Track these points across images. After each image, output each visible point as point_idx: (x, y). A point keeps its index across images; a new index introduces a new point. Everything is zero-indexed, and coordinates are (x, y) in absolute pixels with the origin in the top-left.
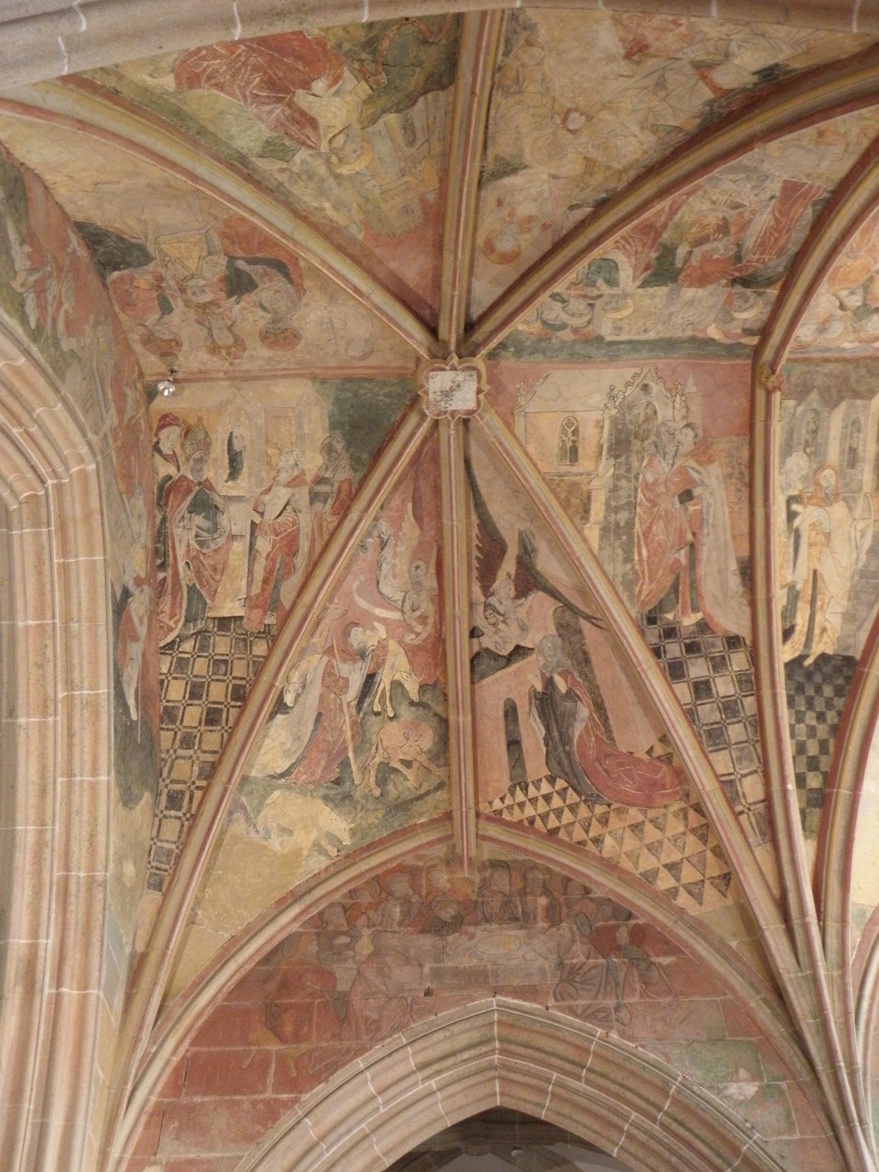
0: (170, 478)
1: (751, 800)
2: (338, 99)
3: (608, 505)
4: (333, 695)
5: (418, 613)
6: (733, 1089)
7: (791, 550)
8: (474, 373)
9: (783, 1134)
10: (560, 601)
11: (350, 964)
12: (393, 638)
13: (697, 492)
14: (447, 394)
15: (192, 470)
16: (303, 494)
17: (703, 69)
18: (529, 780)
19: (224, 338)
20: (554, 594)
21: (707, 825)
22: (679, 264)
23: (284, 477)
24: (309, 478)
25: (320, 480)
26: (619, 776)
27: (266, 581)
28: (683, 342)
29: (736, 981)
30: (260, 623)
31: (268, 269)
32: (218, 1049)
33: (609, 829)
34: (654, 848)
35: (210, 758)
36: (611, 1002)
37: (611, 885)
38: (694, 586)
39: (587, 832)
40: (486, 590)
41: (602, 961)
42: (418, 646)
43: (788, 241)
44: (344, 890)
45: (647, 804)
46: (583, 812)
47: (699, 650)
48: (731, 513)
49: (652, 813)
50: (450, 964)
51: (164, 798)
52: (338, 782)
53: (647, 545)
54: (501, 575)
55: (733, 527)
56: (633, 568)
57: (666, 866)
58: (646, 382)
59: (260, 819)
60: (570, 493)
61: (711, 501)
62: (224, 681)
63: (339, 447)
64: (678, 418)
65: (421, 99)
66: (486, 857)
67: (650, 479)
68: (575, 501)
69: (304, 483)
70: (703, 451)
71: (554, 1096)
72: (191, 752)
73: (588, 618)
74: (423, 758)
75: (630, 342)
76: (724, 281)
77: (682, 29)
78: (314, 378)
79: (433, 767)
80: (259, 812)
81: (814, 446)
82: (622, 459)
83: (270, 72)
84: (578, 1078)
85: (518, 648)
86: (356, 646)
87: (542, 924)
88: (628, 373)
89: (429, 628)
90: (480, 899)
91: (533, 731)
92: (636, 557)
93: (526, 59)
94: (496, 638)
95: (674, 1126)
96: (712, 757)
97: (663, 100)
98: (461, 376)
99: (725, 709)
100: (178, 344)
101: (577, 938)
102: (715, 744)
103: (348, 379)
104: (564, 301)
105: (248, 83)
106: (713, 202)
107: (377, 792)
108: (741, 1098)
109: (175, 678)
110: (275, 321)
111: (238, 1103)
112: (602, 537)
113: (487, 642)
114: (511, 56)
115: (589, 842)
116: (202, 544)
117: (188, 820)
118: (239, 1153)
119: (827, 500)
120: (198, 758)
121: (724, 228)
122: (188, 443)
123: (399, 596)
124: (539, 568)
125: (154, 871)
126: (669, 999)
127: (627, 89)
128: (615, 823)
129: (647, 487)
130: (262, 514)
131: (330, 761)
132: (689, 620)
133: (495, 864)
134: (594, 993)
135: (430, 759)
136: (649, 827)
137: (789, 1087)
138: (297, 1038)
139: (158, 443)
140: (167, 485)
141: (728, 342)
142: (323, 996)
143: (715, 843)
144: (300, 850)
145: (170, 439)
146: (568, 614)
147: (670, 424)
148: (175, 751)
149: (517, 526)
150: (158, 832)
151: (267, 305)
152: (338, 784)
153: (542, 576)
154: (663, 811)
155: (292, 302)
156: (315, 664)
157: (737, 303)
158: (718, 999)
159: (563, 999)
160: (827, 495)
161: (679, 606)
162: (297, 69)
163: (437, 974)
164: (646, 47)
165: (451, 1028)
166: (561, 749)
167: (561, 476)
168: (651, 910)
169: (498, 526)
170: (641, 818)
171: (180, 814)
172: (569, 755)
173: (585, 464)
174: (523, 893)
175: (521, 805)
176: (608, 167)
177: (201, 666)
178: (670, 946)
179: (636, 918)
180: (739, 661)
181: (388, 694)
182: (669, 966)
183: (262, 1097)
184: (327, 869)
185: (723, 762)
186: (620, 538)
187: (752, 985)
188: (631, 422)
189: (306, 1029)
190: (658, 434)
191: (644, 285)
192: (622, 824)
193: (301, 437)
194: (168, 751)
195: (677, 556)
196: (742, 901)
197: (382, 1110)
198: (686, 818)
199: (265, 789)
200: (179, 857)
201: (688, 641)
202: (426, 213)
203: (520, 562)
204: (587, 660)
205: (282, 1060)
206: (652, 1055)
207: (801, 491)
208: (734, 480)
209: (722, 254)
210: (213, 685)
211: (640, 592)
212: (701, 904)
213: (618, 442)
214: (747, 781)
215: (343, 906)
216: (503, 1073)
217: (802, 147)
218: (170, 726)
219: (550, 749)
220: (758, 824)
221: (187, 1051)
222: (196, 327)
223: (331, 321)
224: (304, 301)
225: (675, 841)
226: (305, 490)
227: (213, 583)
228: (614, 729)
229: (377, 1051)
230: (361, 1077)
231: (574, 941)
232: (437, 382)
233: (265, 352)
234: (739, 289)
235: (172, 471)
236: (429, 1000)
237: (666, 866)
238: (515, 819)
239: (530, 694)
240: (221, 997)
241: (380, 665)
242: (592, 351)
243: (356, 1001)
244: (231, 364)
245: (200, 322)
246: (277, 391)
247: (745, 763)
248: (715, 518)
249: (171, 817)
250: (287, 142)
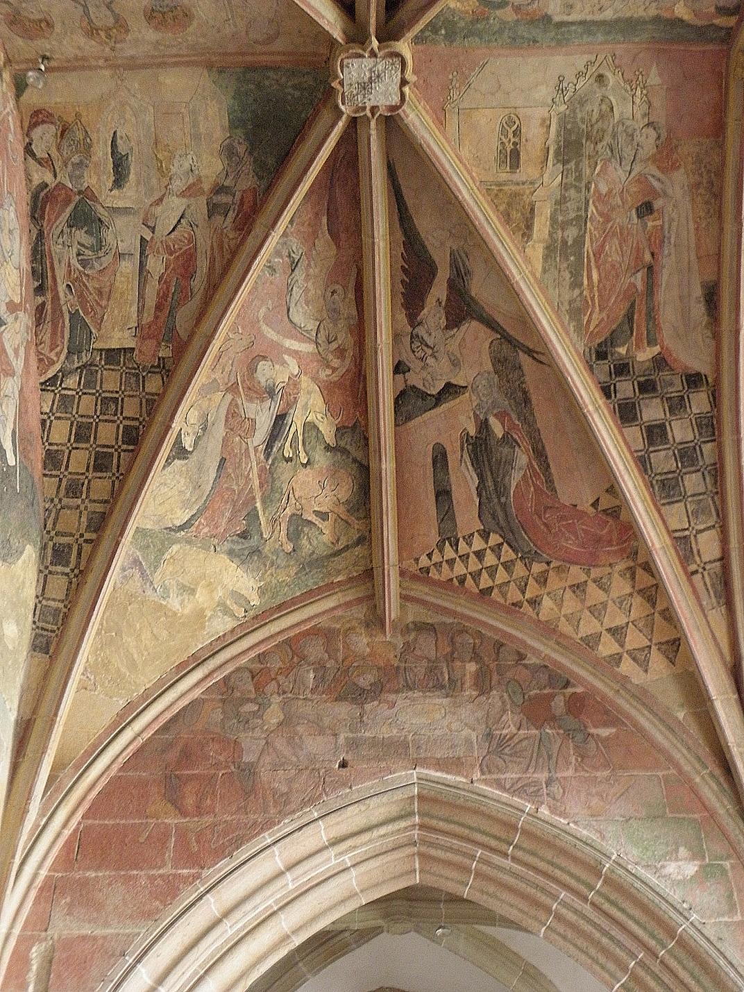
0: (47, 185)
1: (706, 558)
3: (553, 220)
4: (238, 439)
5: (334, 345)
6: (671, 868)
8: (397, 61)
9: (723, 915)
10: (497, 332)
11: (257, 733)
12: (306, 374)
13: (657, 204)
14: (365, 87)
15: (70, 177)
16: (199, 206)
18: (460, 535)
19: (102, 17)
20: (491, 324)
21: (657, 586)
23: (178, 185)
24: (206, 187)
25: (219, 189)
26: (560, 530)
27: (159, 307)
28: (644, 22)
29: (681, 755)
30: (154, 355)
32: (112, 822)
33: (547, 590)
34: (597, 611)
35: (99, 508)
36: (542, 776)
37: (548, 651)
38: (651, 315)
39: (523, 593)
40: (413, 319)
41: (534, 732)
42: (335, 383)
44: (252, 654)
45: (590, 562)
46: (519, 570)
47: (654, 389)
48: (697, 229)
49: (595, 573)
50: (367, 734)
51: (50, 551)
52: (244, 535)
53: (598, 267)
54: (431, 301)
55: (698, 247)
56: (581, 293)
57: (609, 630)
59: (157, 577)
60: (509, 204)
61: (674, 215)
62: (114, 422)
63: (241, 149)
64: (638, 116)
66: (410, 619)
67: (604, 189)
68: (516, 215)
69: (203, 193)
70: (666, 156)
71: (478, 874)
72: (79, 501)
73: (530, 352)
74: (342, 510)
78: (209, 66)
79: (352, 519)
80: (156, 568)
82: (572, 165)
84: (505, 855)
85: (449, 385)
86: (263, 383)
87: (470, 692)
88: (580, 61)
89: (348, 361)
90: (403, 665)
91: (464, 480)
92: (585, 282)
94: (424, 374)
95: (606, 906)
96: (663, 509)
99: (681, 457)
101: (508, 706)
102: (668, 496)
103: (251, 68)
107: (289, 547)
108: (680, 877)
109: (59, 418)
111: (136, 878)
112: (546, 258)
113: (414, 379)
115: (525, 603)
116: (84, 263)
117: (76, 576)
118: (137, 930)
120: (86, 508)
122: (65, 143)
123: (312, 326)
124: (473, 294)
125: (40, 631)
126: (606, 773)
128: (554, 582)
129: (600, 198)
130: (153, 230)
131: (234, 514)
132: (645, 355)
133: (420, 627)
134: (524, 766)
135: (348, 511)
136: (592, 587)
137: (733, 867)
138: (199, 811)
139: (31, 144)
140: (42, 194)
141: (699, 23)
142: (227, 767)
143: (665, 605)
144: (203, 610)
145: (44, 138)
146: (506, 348)
147: (628, 123)
148: (60, 500)
149: (448, 244)
150: (44, 590)
152: (245, 538)
153: (477, 304)
154: (608, 570)
156: (219, 403)
158: (660, 774)
159: (490, 772)
161: (633, 338)
163: (353, 744)
165: (367, 801)
166: (496, 500)
167: (500, 185)
168: (591, 679)
169: (426, 243)
170: (583, 577)
171: (67, 570)
172: (504, 507)
173: (528, 171)
174: (450, 658)
175: (451, 562)
177: (87, 405)
178: (610, 716)
179: (574, 686)
180: (699, 402)
181: (301, 438)
182: (607, 738)
183: (161, 871)
184: (233, 630)
185: (677, 516)
186: (567, 259)
187: (699, 759)
188: (583, 120)
189: (209, 801)
190: (614, 136)
192: (563, 584)
193: (197, 137)
194: (52, 500)
195: (633, 279)
196: (691, 669)
197: (291, 887)
198: (633, 578)
199: (163, 544)
200: (66, 616)
201: (642, 379)
203: (451, 285)
204: (527, 401)
205: (182, 834)
206: (585, 832)
208: (701, 191)
210: (101, 425)
211: (589, 322)
212: (646, 671)
213: (568, 144)
214: (702, 538)
215: (251, 672)
216: (423, 849)
218: (54, 473)
219: (484, 500)
220: (713, 585)
221: (79, 823)
225: (621, 603)
226: (203, 200)
227: (98, 309)
228: (555, 477)
229: (286, 826)
230: (268, 852)
231: (504, 711)
233: (151, 35)
235: (48, 178)
236: (344, 771)
237: (609, 630)
238: (443, 578)
239: (462, 438)
240: (115, 767)
241: (291, 404)
242: (536, 33)
243: (264, 775)
244: (113, 49)
246: (168, 81)
247: (702, 517)
248: (678, 236)
249: (57, 573)
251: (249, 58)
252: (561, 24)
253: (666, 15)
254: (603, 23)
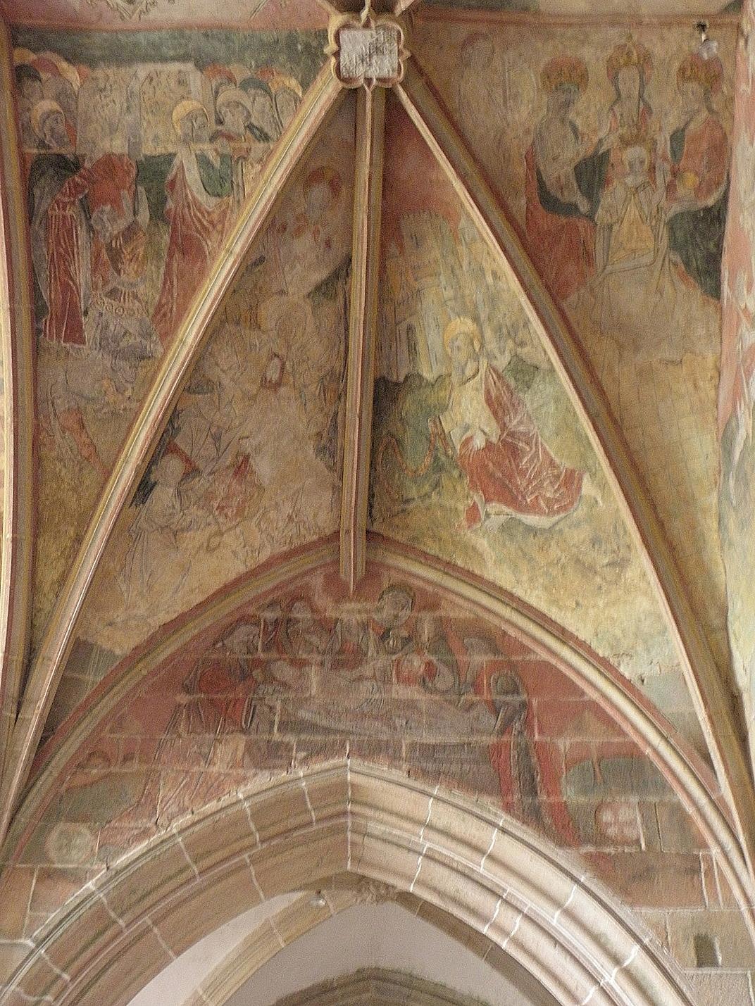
2: (467, 420)
14: (377, 49)
17: (192, 471)
19: (629, 79)
22: (141, 189)
28: (103, 58)
31: (559, 195)
43: (47, 239)
58: (132, 7)
65: (402, 379)
75: (164, 60)
76: (87, 165)
77: (216, 505)
78: (537, 13)
83: (514, 466)
88: (154, 14)
93: (320, 417)
97: (211, 423)
98: (360, 71)
100: (682, 71)
104: (250, 127)
105: (531, 460)
106: (136, 297)
110: (567, 104)
114: (331, 414)
121: (116, 257)
127: (241, 424)
141: (49, 55)
151: (571, 136)
155: (542, 139)
157: (61, 128)
162: (494, 464)
164: (236, 473)
176: (238, 323)
191: (170, 157)
202: (398, 228)
209: (102, 212)
217: (90, 400)
222: (654, 102)
223: (505, 102)
224: (530, 140)
232: (388, 65)
234: (68, 151)
244: (631, 37)
245: (648, 110)
250: (512, 383)
251: (496, 16)
252: (184, 58)
253: (85, 69)
254: (145, 59)
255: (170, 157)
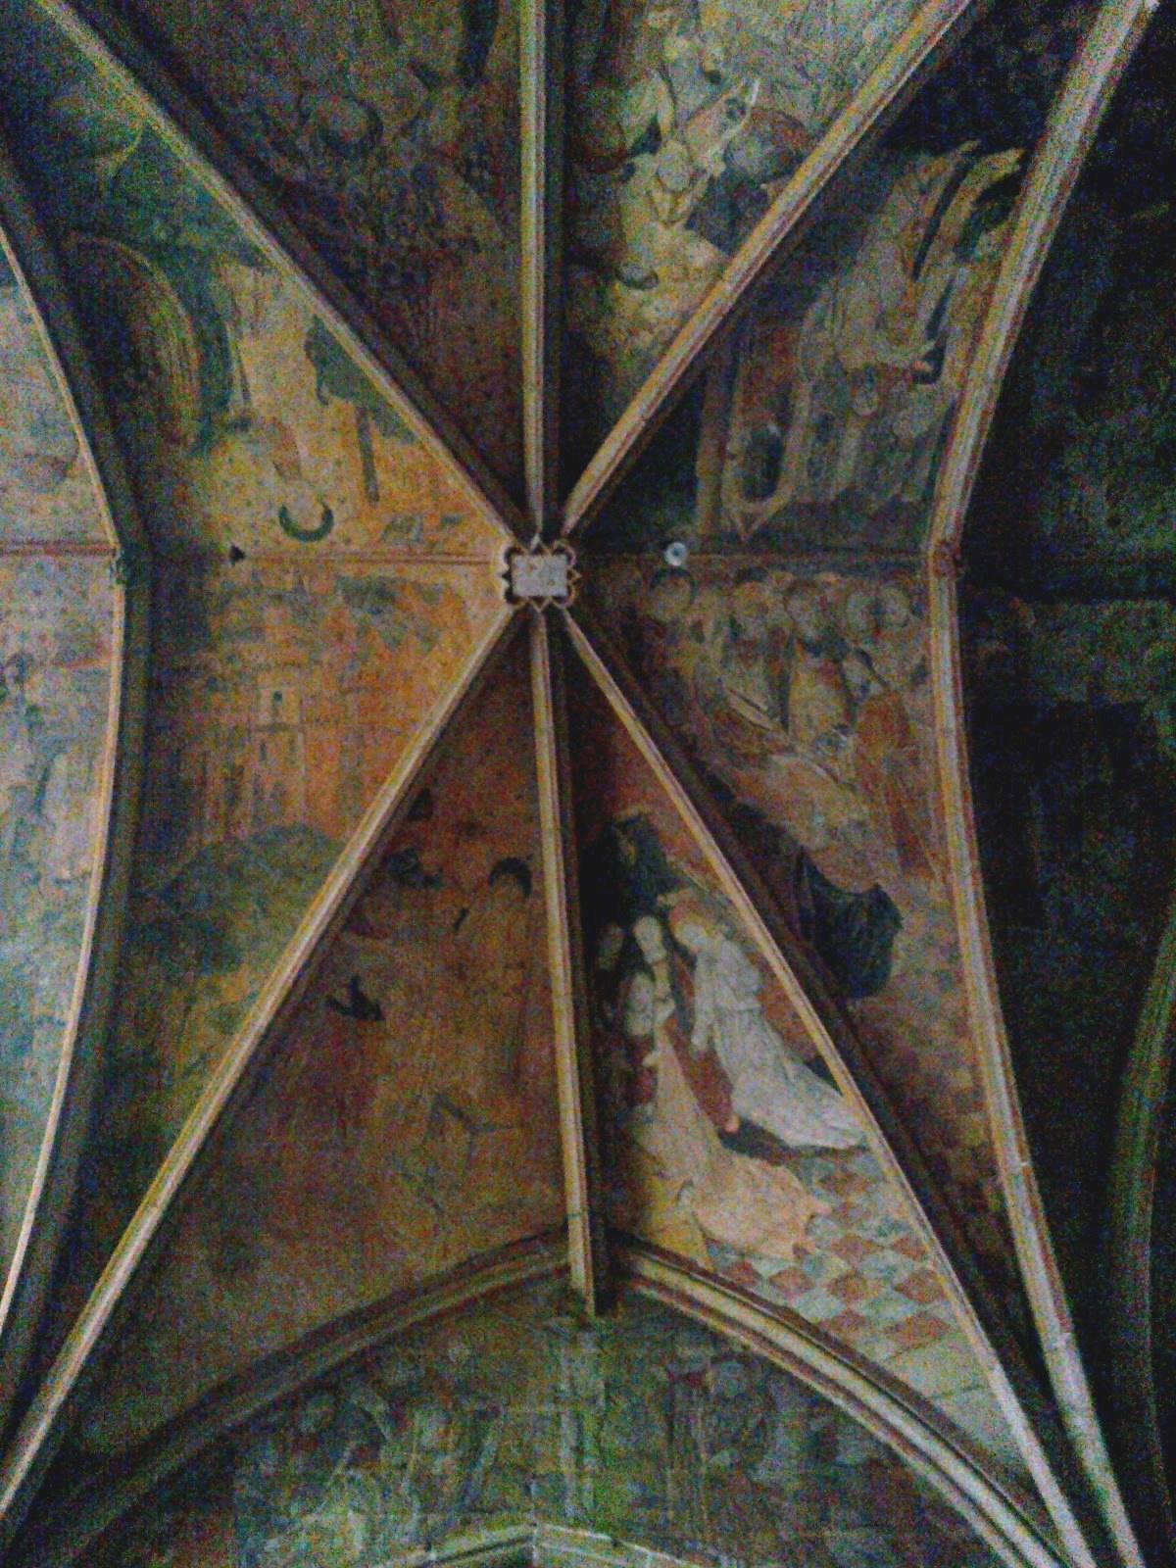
7: (949, 306)
75: (1136, 596)
81: (880, 446)
119: (873, 374)
160: (871, 381)
190: (1113, 465)
191: (1137, 707)
207: (910, 389)
254: (1114, 595)
255: (1137, 707)
